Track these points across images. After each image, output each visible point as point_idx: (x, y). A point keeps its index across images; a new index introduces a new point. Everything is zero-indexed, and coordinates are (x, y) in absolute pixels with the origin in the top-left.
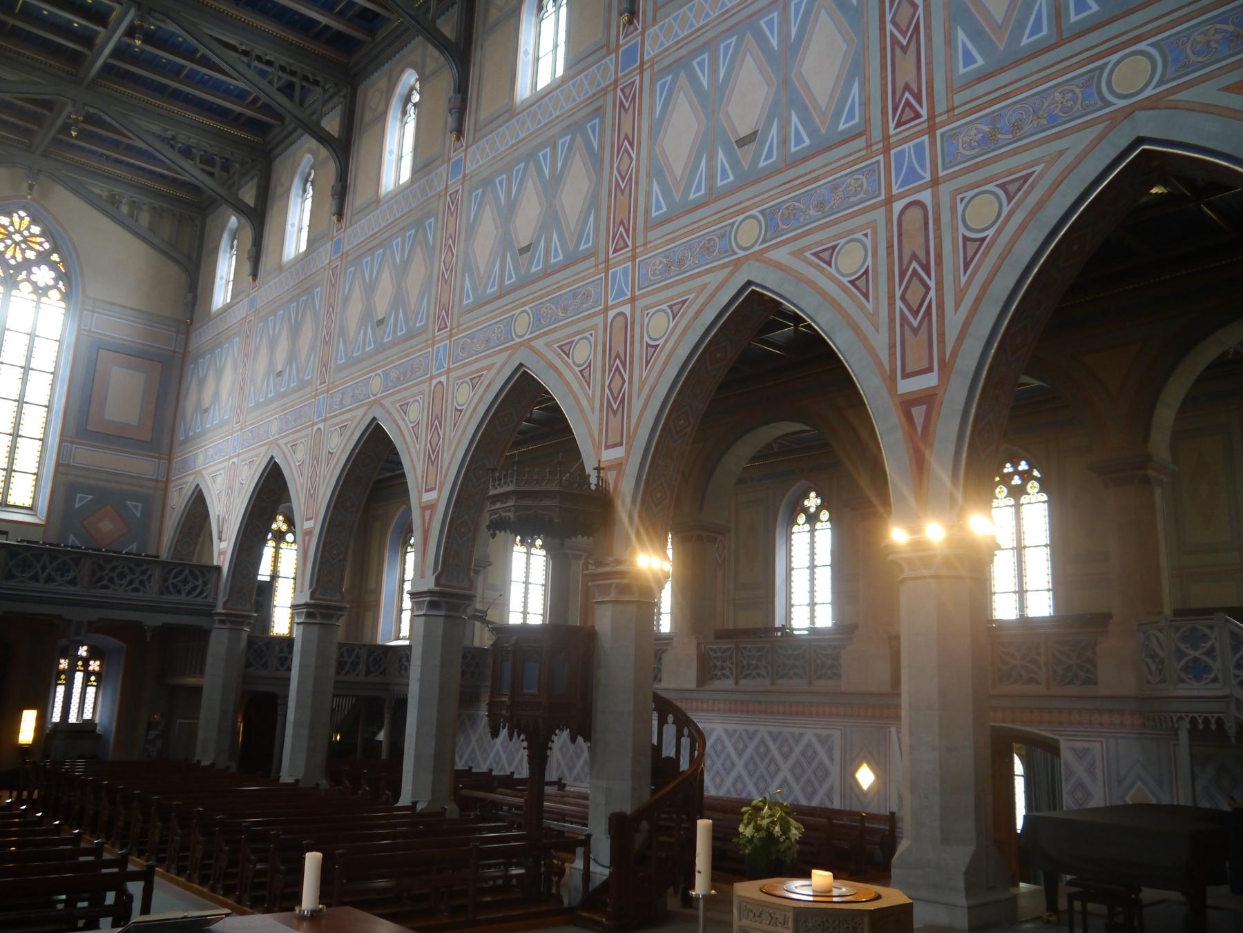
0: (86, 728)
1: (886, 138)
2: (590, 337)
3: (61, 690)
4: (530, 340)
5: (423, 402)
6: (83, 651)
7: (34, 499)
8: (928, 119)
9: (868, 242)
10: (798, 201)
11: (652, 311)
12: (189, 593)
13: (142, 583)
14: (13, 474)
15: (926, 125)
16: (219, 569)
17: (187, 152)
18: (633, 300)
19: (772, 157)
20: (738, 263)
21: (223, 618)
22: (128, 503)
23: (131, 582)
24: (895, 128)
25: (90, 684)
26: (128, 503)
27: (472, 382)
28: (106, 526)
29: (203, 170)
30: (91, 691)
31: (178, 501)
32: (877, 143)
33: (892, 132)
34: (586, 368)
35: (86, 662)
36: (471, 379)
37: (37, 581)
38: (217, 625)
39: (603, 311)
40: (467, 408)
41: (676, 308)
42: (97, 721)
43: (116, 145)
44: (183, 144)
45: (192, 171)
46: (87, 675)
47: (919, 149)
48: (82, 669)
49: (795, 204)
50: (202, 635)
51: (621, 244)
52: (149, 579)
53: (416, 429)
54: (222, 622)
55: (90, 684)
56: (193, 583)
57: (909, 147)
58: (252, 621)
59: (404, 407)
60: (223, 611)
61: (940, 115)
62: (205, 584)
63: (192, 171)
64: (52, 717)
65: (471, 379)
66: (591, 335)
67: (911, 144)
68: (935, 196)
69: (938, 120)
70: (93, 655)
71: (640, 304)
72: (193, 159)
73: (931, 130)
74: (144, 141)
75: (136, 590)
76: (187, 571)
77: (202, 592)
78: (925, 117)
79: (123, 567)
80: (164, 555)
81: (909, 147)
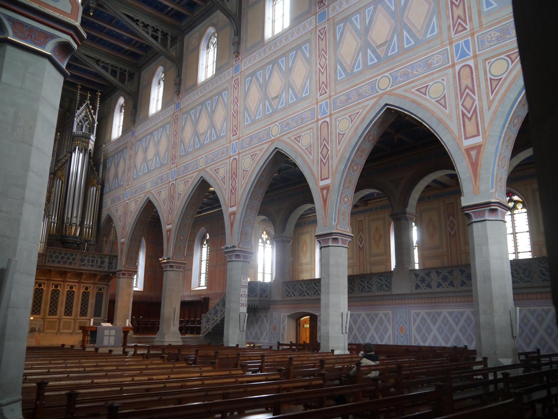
1: (450, 39)
2: (310, 133)
4: (279, 137)
5: (313, 134)
8: (470, 30)
9: (311, 134)
10: (408, 68)
11: (340, 119)
15: (469, 33)
18: (331, 115)
19: (360, 67)
20: (381, 96)
24: (454, 35)
27: (351, 118)
32: (446, 41)
33: (453, 36)
34: (309, 147)
36: (251, 156)
39: (456, 65)
40: (250, 170)
41: (353, 117)
47: (467, 43)
49: (407, 70)
51: (235, 133)
53: (223, 179)
57: (462, 42)
59: (217, 171)
61: (476, 28)
65: (251, 156)
66: (311, 132)
67: (463, 41)
68: (331, 120)
69: (475, 30)
71: (334, 117)
73: (472, 35)
78: (469, 30)
81: (462, 42)
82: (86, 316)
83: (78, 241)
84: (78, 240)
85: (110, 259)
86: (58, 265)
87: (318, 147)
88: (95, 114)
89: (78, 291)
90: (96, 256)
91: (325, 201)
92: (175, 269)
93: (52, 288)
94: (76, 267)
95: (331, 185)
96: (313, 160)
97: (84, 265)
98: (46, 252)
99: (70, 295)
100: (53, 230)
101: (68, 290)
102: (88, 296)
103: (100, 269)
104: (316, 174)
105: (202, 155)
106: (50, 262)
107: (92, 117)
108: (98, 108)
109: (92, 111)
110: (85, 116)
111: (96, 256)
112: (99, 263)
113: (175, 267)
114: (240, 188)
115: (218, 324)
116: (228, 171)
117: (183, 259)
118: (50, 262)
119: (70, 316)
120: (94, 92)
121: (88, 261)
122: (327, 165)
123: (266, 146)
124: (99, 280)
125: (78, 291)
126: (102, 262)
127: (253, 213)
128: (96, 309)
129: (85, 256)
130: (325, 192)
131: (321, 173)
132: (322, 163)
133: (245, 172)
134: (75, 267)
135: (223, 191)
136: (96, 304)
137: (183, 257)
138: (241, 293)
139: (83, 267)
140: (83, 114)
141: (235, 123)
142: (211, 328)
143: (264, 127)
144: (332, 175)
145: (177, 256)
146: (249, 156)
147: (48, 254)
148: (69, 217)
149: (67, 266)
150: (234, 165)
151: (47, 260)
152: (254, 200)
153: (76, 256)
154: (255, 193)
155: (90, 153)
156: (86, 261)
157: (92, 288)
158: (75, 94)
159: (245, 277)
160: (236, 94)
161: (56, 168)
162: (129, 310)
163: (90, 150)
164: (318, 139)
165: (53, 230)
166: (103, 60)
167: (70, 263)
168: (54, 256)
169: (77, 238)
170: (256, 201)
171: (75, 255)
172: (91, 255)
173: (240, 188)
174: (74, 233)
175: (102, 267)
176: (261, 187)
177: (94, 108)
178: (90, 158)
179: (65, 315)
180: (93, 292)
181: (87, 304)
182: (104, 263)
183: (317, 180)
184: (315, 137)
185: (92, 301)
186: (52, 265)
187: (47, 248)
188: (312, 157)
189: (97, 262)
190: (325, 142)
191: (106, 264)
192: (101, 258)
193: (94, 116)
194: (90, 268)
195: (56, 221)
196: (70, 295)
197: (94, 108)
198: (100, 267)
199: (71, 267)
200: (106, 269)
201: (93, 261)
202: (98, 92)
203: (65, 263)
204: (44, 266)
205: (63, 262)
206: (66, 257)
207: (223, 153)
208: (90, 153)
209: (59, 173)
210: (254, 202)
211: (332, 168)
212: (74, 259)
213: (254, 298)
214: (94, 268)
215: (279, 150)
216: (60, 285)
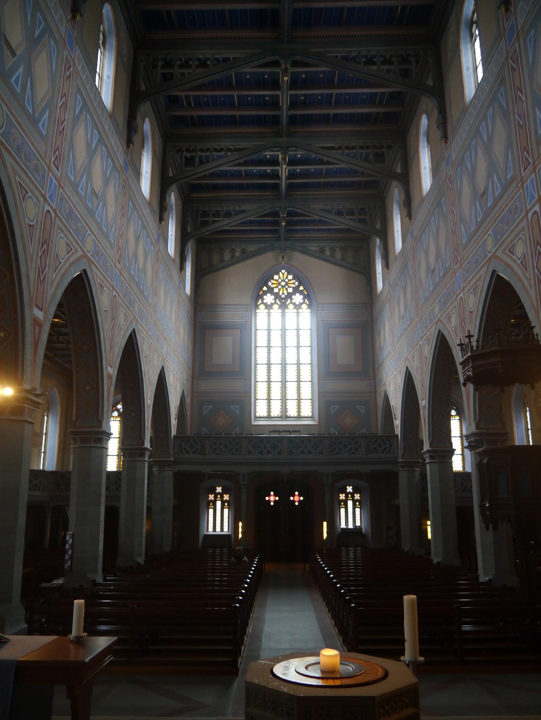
0: (357, 531)
3: (343, 510)
6: (219, 490)
7: (313, 412)
12: (383, 452)
13: (356, 449)
14: (301, 401)
16: (397, 436)
17: (339, 213)
21: (402, 464)
22: (357, 407)
23: (350, 449)
25: (356, 506)
26: (357, 407)
28: (348, 421)
29: (351, 219)
30: (358, 510)
31: (380, 401)
35: (222, 495)
37: (304, 454)
38: (400, 469)
42: (363, 527)
43: (307, 223)
44: (336, 209)
45: (344, 222)
46: (354, 502)
48: (351, 499)
50: (395, 475)
52: (360, 446)
54: (403, 467)
55: (356, 506)
56: (384, 446)
58: (420, 464)
60: (402, 460)
62: (391, 446)
63: (344, 222)
64: (340, 525)
70: (224, 491)
72: (343, 215)
74: (317, 215)
75: (353, 453)
76: (379, 440)
77: (390, 451)
79: (345, 441)
80: (380, 433)
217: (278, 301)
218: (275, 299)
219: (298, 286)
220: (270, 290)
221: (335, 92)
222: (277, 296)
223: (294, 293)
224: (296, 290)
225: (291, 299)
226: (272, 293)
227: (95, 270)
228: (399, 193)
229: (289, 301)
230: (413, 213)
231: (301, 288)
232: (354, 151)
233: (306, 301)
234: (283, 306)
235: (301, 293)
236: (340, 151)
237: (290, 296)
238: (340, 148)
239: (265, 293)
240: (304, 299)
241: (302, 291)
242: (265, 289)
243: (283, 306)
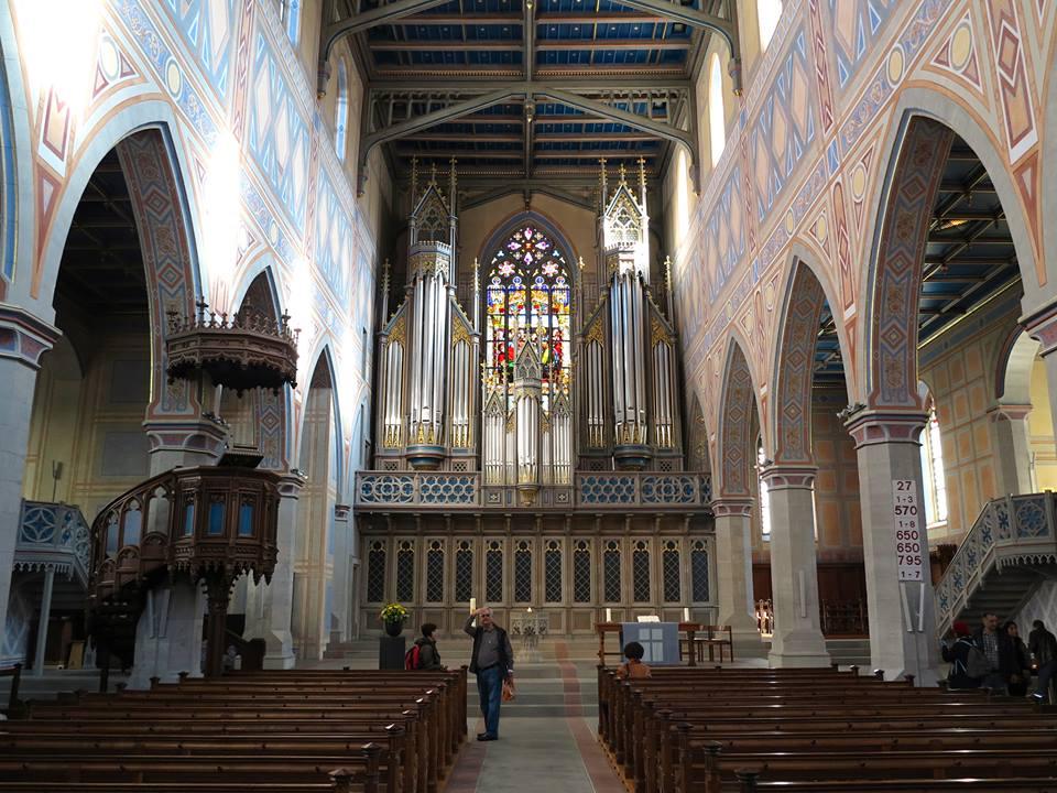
82: (679, 600)
83: (644, 454)
84: (646, 451)
85: (702, 481)
86: (601, 505)
87: (990, 50)
88: (640, 202)
89: (655, 552)
90: (673, 478)
91: (1031, 204)
92: (786, 485)
93: (546, 548)
94: (637, 503)
95: (1039, 147)
96: (985, 97)
97: (652, 499)
98: (575, 483)
99: (641, 560)
100: (599, 439)
101: (608, 552)
102: (676, 560)
103: (687, 504)
104: (997, 133)
105: (787, 207)
106: (586, 499)
107: (636, 210)
108: (644, 190)
109: (634, 199)
110: (624, 212)
111: (673, 478)
112: (681, 490)
113: (786, 480)
114: (855, 254)
115: (964, 610)
116: (831, 222)
117: (806, 459)
118: (586, 499)
119: (498, 601)
120: (631, 163)
121: (658, 490)
122: (1020, 90)
123: (885, 120)
124: (691, 526)
125: (655, 552)
126: (688, 490)
127: (903, 309)
128: (695, 585)
129: (651, 480)
130: (1027, 176)
131: (1009, 123)
132: (1006, 90)
133: (858, 208)
134: (633, 505)
135: (830, 272)
136: (694, 576)
137: (805, 455)
138: (898, 528)
139: (649, 504)
140: (619, 210)
141: (825, 98)
142: (952, 619)
143: (874, 71)
144: (1037, 112)
145: (788, 455)
146: (860, 163)
147: (580, 486)
148: (622, 409)
149: (618, 504)
150: (838, 201)
151: (579, 497)
152: (893, 275)
153: (633, 483)
154: (893, 255)
155: (641, 280)
156: (654, 490)
157: (651, 542)
158: (597, 178)
159: (906, 485)
160: (816, 28)
161: (585, 323)
162: (744, 586)
163: (640, 273)
164: (986, 24)
165: (599, 439)
166: (616, 92)
167: (624, 498)
168: (431, 487)
169: (641, 447)
170: (902, 275)
171: (630, 480)
172: (663, 478)
173: (855, 254)
174: (635, 439)
175: (688, 499)
176: (904, 235)
177: (637, 192)
178: (644, 289)
179: (666, 600)
180: (684, 550)
181: (677, 577)
182: (692, 490)
183: (1002, 149)
184: (980, 23)
185: (685, 569)
186: (590, 504)
187: (575, 474)
188: (980, 89)
189: (677, 490)
190: (1004, 23)
191: (696, 492)
192: (683, 481)
193: (639, 207)
194: (663, 503)
195: (602, 423)
196: (641, 560)
197: (637, 192)
198: (684, 499)
199: (627, 505)
200: (698, 502)
201: (667, 490)
202: (639, 159)
203: (613, 498)
204: (575, 509)
205: (622, 498)
206: (603, 488)
207: (817, 181)
208: (641, 280)
209: (593, 333)
210: (898, 279)
211: (1036, 90)
212: (630, 490)
213: (1040, 537)
214: (673, 503)
215: (914, 114)
216: (619, 542)
217: (520, 272)
218: (516, 269)
219: (550, 251)
220: (509, 258)
221: (596, 22)
222: (520, 264)
223: (544, 261)
224: (548, 253)
225: (541, 270)
226: (511, 260)
227: (279, 266)
228: (686, 157)
229: (537, 272)
230: (702, 185)
231: (556, 253)
232: (625, 101)
233: (563, 272)
234: (529, 280)
235: (556, 260)
236: (605, 101)
237: (538, 265)
238: (606, 97)
239: (501, 262)
240: (560, 269)
241: (558, 258)
242: (501, 254)
243: (529, 280)
